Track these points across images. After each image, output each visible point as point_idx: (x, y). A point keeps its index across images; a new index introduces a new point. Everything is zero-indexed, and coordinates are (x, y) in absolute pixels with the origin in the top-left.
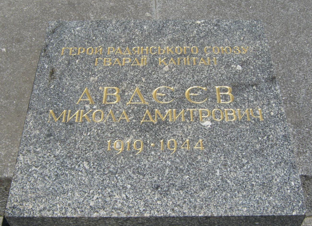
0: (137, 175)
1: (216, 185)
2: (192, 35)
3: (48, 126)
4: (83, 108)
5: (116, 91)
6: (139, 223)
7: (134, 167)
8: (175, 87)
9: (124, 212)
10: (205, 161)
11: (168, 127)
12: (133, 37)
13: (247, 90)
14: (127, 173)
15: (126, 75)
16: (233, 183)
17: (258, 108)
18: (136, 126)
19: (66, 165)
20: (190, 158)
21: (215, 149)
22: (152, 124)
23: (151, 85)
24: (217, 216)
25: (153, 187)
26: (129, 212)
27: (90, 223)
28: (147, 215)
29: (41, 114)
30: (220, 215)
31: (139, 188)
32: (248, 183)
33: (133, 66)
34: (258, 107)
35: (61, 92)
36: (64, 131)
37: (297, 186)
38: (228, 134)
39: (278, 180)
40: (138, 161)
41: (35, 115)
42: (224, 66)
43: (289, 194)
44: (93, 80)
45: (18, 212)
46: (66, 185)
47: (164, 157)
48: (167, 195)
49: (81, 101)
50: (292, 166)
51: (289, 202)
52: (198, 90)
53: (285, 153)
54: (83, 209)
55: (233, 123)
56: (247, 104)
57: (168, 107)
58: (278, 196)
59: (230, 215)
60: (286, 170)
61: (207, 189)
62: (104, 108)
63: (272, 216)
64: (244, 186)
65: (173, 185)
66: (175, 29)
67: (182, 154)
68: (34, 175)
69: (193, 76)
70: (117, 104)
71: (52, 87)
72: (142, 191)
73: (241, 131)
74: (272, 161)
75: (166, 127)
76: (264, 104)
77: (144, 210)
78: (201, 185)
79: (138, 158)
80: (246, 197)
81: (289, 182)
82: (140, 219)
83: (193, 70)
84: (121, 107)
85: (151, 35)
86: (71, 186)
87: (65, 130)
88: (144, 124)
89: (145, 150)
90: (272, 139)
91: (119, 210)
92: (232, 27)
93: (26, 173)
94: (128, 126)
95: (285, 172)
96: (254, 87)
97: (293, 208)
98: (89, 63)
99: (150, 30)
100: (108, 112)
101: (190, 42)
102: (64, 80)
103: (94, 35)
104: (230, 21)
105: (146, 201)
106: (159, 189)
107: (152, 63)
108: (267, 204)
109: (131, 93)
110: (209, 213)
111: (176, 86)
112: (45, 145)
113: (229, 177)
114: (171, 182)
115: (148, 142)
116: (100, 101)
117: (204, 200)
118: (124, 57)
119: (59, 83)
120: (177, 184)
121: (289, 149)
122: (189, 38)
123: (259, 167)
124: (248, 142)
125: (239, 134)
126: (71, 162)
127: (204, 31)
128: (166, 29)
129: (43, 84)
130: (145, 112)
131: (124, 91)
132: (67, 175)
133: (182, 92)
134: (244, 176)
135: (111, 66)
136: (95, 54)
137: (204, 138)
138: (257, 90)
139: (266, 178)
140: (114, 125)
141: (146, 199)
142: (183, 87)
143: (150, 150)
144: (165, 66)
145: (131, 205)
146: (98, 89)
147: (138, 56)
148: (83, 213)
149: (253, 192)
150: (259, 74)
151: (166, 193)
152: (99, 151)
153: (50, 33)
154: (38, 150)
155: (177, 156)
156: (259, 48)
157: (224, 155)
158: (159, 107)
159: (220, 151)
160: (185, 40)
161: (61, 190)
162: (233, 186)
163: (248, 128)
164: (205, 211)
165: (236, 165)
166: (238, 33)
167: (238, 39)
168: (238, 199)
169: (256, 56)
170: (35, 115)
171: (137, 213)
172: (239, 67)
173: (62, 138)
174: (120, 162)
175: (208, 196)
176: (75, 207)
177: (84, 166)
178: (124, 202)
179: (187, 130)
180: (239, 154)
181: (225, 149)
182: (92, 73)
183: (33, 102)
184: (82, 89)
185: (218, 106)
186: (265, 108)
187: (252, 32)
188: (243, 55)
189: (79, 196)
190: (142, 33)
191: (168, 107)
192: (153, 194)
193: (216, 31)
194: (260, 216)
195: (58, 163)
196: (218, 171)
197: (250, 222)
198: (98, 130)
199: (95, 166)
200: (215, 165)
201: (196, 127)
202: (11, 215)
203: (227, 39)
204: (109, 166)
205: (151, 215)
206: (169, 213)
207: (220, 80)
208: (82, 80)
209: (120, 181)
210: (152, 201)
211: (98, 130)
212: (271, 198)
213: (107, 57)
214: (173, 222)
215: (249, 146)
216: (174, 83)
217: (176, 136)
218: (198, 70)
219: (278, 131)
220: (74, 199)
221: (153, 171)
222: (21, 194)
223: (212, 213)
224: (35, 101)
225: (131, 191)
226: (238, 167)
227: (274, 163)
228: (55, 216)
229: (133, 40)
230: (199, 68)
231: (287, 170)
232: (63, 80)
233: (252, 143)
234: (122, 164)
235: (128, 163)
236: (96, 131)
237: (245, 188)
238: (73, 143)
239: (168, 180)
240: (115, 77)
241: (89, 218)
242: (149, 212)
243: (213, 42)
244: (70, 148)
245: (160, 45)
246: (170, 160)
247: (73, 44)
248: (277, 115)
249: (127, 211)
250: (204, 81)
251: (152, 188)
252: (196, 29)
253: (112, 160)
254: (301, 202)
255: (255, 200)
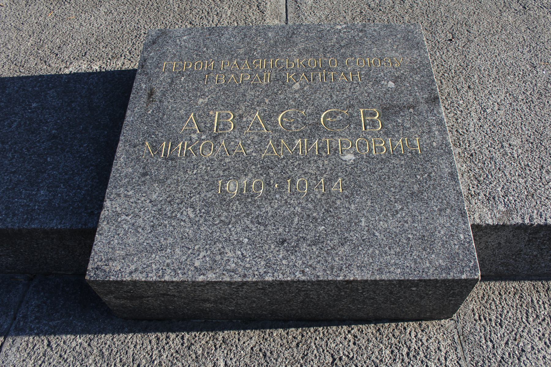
0: (257, 225)
1: (360, 238)
2: (330, 44)
3: (143, 162)
4: (188, 138)
6: (259, 289)
7: (253, 216)
8: (308, 110)
9: (239, 275)
10: (347, 206)
11: (297, 162)
12: (255, 47)
13: (402, 114)
14: (243, 223)
15: (245, 95)
16: (382, 236)
17: (416, 137)
18: (256, 161)
19: (165, 212)
20: (327, 203)
21: (360, 191)
22: (276, 159)
23: (277, 107)
24: (361, 280)
25: (277, 242)
26: (246, 275)
27: (195, 289)
28: (269, 278)
29: (135, 147)
30: (365, 278)
31: (260, 243)
32: (403, 235)
34: (416, 135)
35: (161, 119)
36: (164, 169)
37: (468, 240)
38: (376, 172)
39: (442, 233)
40: (258, 207)
41: (127, 148)
42: (371, 83)
43: (457, 251)
44: (202, 103)
45: (103, 274)
46: (165, 239)
47: (292, 202)
48: (296, 251)
49: (186, 130)
50: (461, 213)
51: (457, 261)
52: (337, 114)
53: (451, 196)
54: (186, 271)
55: (384, 157)
56: (401, 132)
58: (442, 253)
59: (378, 279)
60: (453, 218)
61: (348, 243)
62: (215, 138)
63: (434, 280)
64: (398, 240)
65: (304, 239)
66: (308, 37)
67: (316, 197)
68: (124, 226)
69: (331, 96)
71: (150, 112)
72: (262, 247)
73: (394, 167)
74: (434, 207)
75: (296, 162)
76: (424, 132)
77: (265, 272)
78: (341, 238)
79: (258, 203)
80: (400, 254)
81: (457, 235)
82: (260, 284)
83: (331, 88)
84: (237, 136)
85: (278, 44)
86: (170, 240)
87: (165, 167)
88: (267, 159)
89: (267, 192)
90: (435, 177)
91: (233, 272)
92: (382, 33)
93: (114, 224)
94: (246, 161)
95: (452, 221)
96: (411, 110)
97: (462, 270)
98: (198, 80)
99: (276, 37)
100: (221, 143)
101: (328, 53)
102: (166, 103)
103: (205, 46)
104: (380, 26)
105: (268, 261)
106: (286, 245)
107: (278, 80)
108: (428, 265)
109: (251, 119)
110: (351, 276)
111: (309, 109)
112: (139, 187)
113: (377, 228)
114: (301, 235)
115: (272, 182)
116: (211, 129)
117: (344, 258)
120: (309, 237)
121: (457, 191)
122: (326, 48)
123: (417, 214)
124: (403, 181)
125: (391, 171)
126: (172, 209)
127: (345, 38)
128: (296, 37)
129: (138, 109)
130: (269, 142)
131: (241, 116)
132: (166, 226)
133: (317, 116)
134: (397, 227)
135: (225, 85)
137: (345, 176)
138: (415, 114)
139: (427, 230)
140: (227, 160)
141: (268, 257)
142: (318, 110)
143: (274, 192)
144: (294, 83)
145: (248, 266)
146: (209, 114)
147: (261, 71)
148: (186, 276)
149: (409, 248)
150: (417, 94)
151: (294, 250)
152: (207, 194)
153: (149, 44)
154: (129, 194)
155: (310, 200)
156: (417, 59)
157: (372, 199)
158: (287, 136)
159: (366, 194)
160: (321, 50)
161: (158, 245)
162: (383, 240)
163: (403, 162)
164: (345, 273)
165: (386, 212)
166: (390, 41)
167: (390, 49)
168: (389, 257)
169: (413, 69)
170: (127, 148)
171: (256, 276)
172: (391, 84)
173: (161, 178)
174: (234, 208)
175: (350, 254)
176: (175, 268)
177: (188, 214)
178: (239, 261)
179: (323, 166)
180: (391, 198)
181: (373, 190)
182: (201, 94)
183: (125, 132)
185: (364, 135)
186: (426, 136)
187: (408, 40)
188: (396, 69)
189: (181, 253)
190: (266, 41)
191: (298, 137)
192: (277, 251)
193: (361, 38)
194: (418, 280)
195: (154, 211)
196: (363, 220)
197: (404, 288)
198: (207, 167)
199: (201, 214)
200: (359, 212)
201: (335, 162)
202: (94, 278)
203: (375, 49)
204: (220, 213)
205: (274, 279)
206: (297, 276)
207: (366, 101)
208: (188, 102)
209: (234, 233)
210: (275, 260)
211: (207, 167)
212: (433, 256)
213: (221, 72)
214: (303, 287)
215: (403, 186)
216: (307, 105)
217: (309, 174)
218: (338, 88)
219: (442, 167)
220: (175, 258)
221: (278, 220)
222: (107, 250)
223: (354, 275)
224: (128, 131)
225: (248, 247)
226: (389, 214)
227: (436, 209)
228: (149, 279)
229: (254, 51)
230: (339, 86)
231: (455, 218)
232: (165, 103)
233: (408, 182)
234: (237, 211)
235: (245, 209)
236: (204, 168)
237: (398, 243)
238: (174, 183)
239: (297, 233)
240: (230, 98)
241: (193, 282)
242: (271, 275)
243: (357, 52)
244: (171, 190)
246: (300, 205)
247: (177, 57)
248: (441, 145)
249: (242, 273)
250: (345, 103)
251: (276, 243)
252: (336, 36)
253: (224, 206)
254: (472, 261)
255: (411, 258)
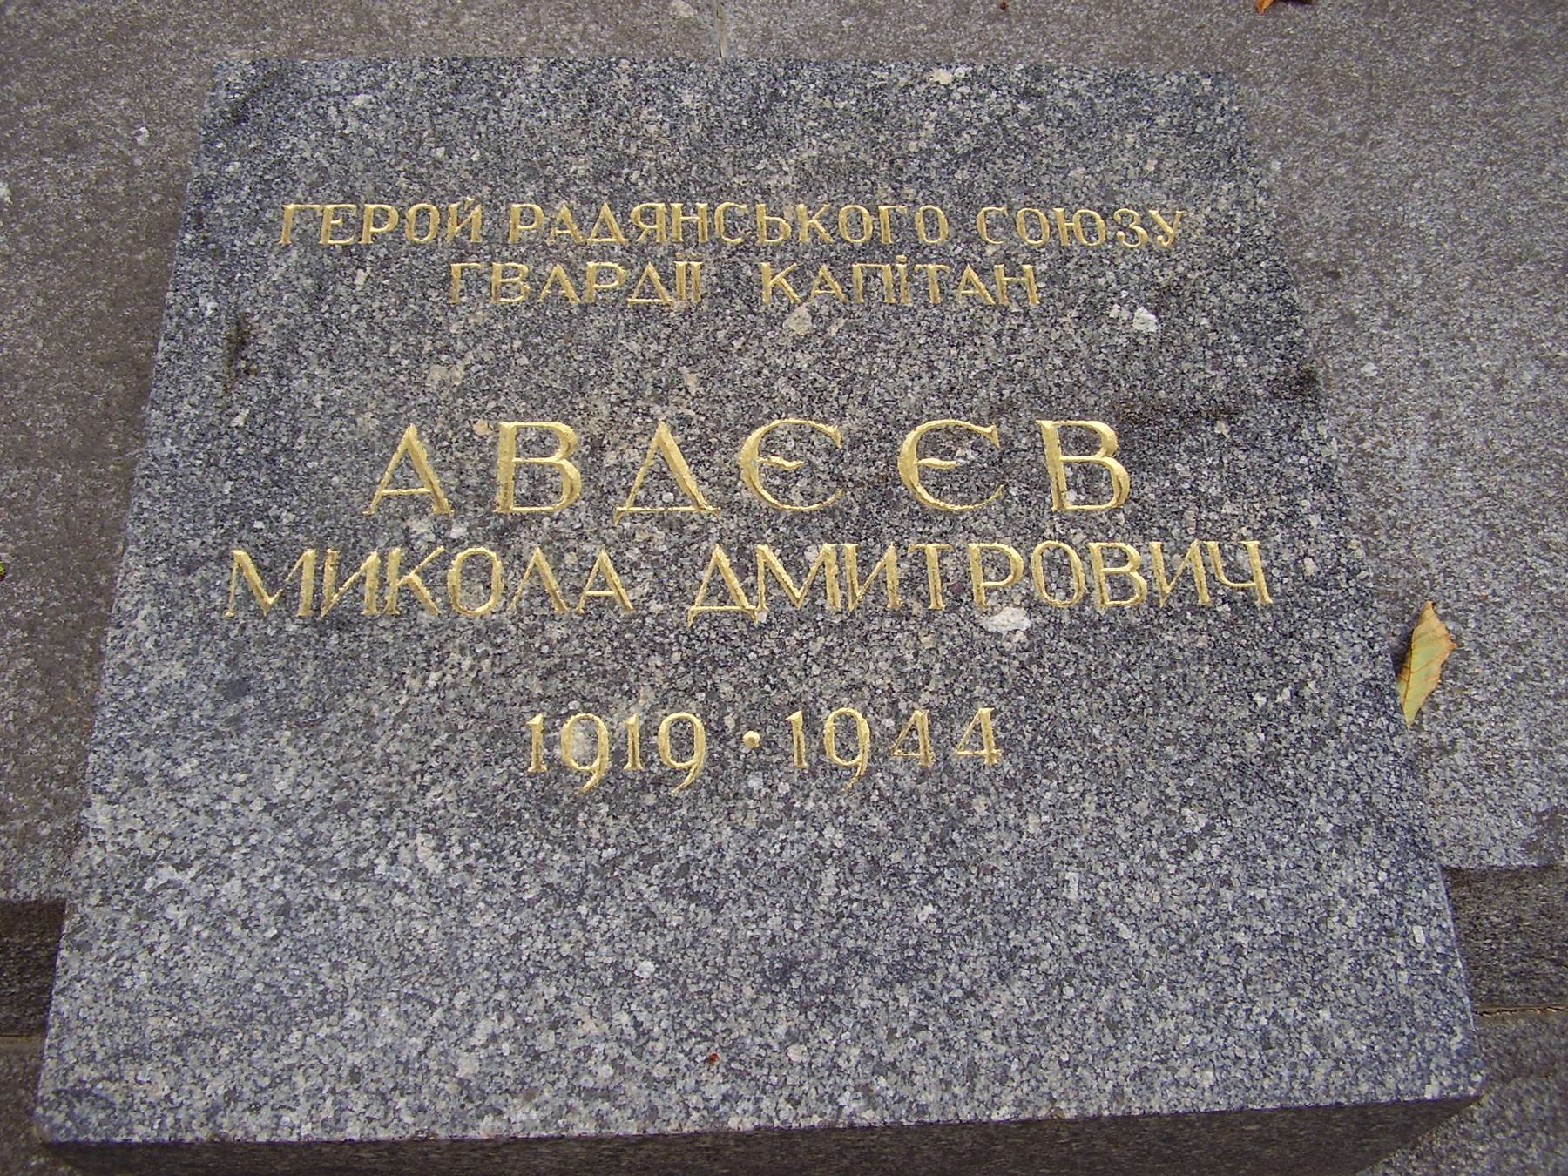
5: (556, 440)
8: (846, 423)
12: (632, 151)
15: (607, 356)
33: (636, 309)
57: (816, 533)
70: (567, 513)
71: (239, 421)
102: (300, 383)
107: (728, 293)
109: (634, 455)
116: (484, 500)
118: (589, 257)
119: (276, 401)
136: (449, 239)
144: (791, 309)
184: (389, 435)
190: (673, 127)
191: (816, 533)
245: (766, 193)
247: (335, 183)
